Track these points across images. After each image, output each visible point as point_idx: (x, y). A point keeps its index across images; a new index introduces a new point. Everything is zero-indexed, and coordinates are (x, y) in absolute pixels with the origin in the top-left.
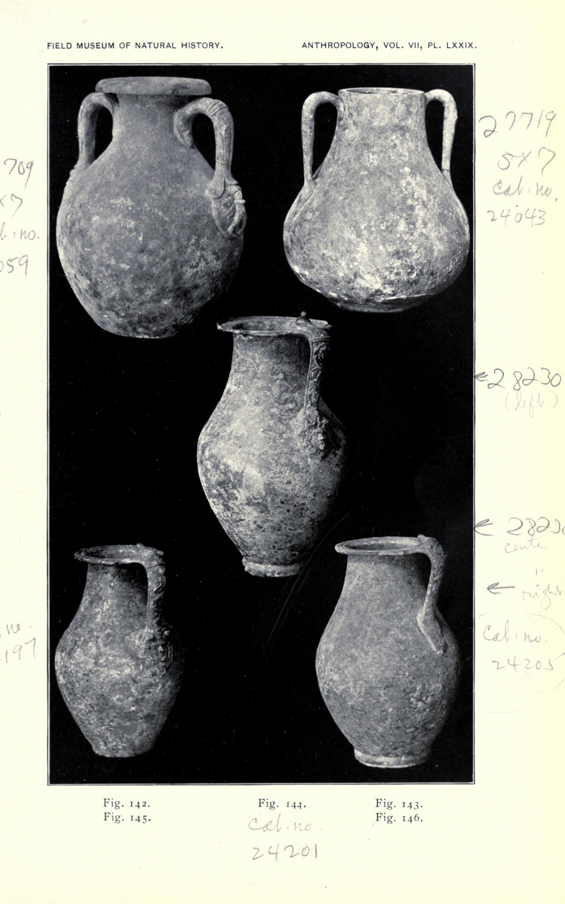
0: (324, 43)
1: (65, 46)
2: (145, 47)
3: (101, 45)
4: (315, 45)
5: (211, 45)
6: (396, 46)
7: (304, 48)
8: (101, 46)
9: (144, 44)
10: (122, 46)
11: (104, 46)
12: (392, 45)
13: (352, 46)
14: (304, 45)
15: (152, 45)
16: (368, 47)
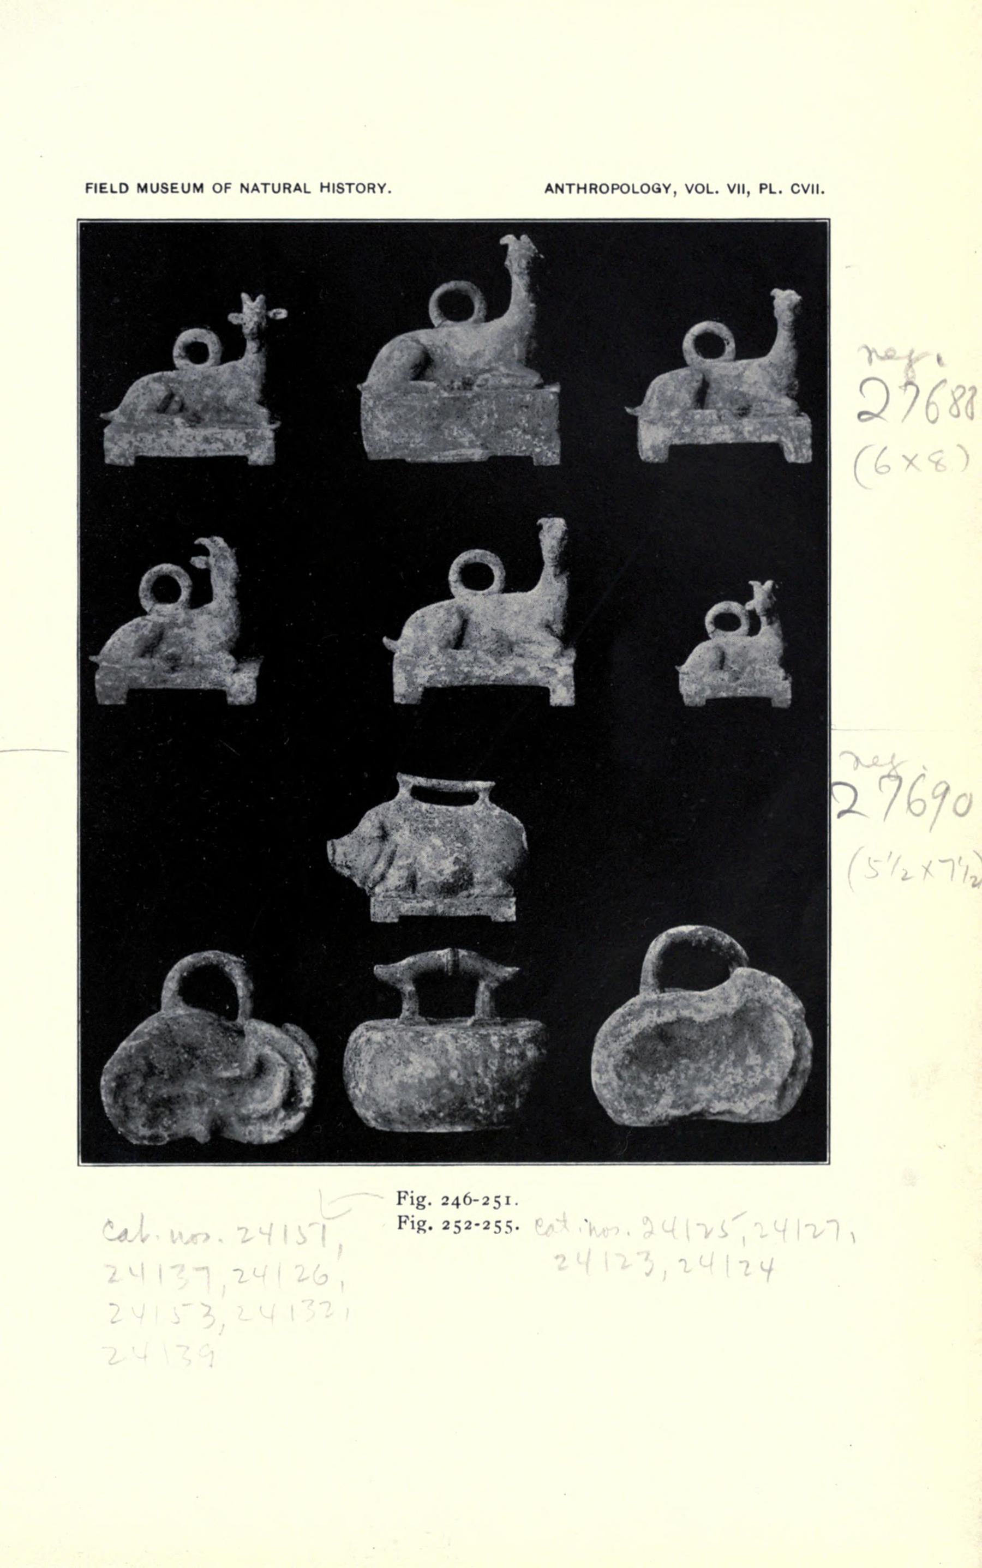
0: (582, 186)
1: (116, 188)
2: (257, 190)
3: (179, 187)
4: (566, 188)
5: (371, 187)
6: (706, 189)
7: (549, 192)
8: (179, 189)
9: (255, 185)
10: (218, 188)
11: (186, 189)
12: (700, 189)
13: (631, 189)
14: (549, 188)
15: (269, 188)
16: (659, 190)
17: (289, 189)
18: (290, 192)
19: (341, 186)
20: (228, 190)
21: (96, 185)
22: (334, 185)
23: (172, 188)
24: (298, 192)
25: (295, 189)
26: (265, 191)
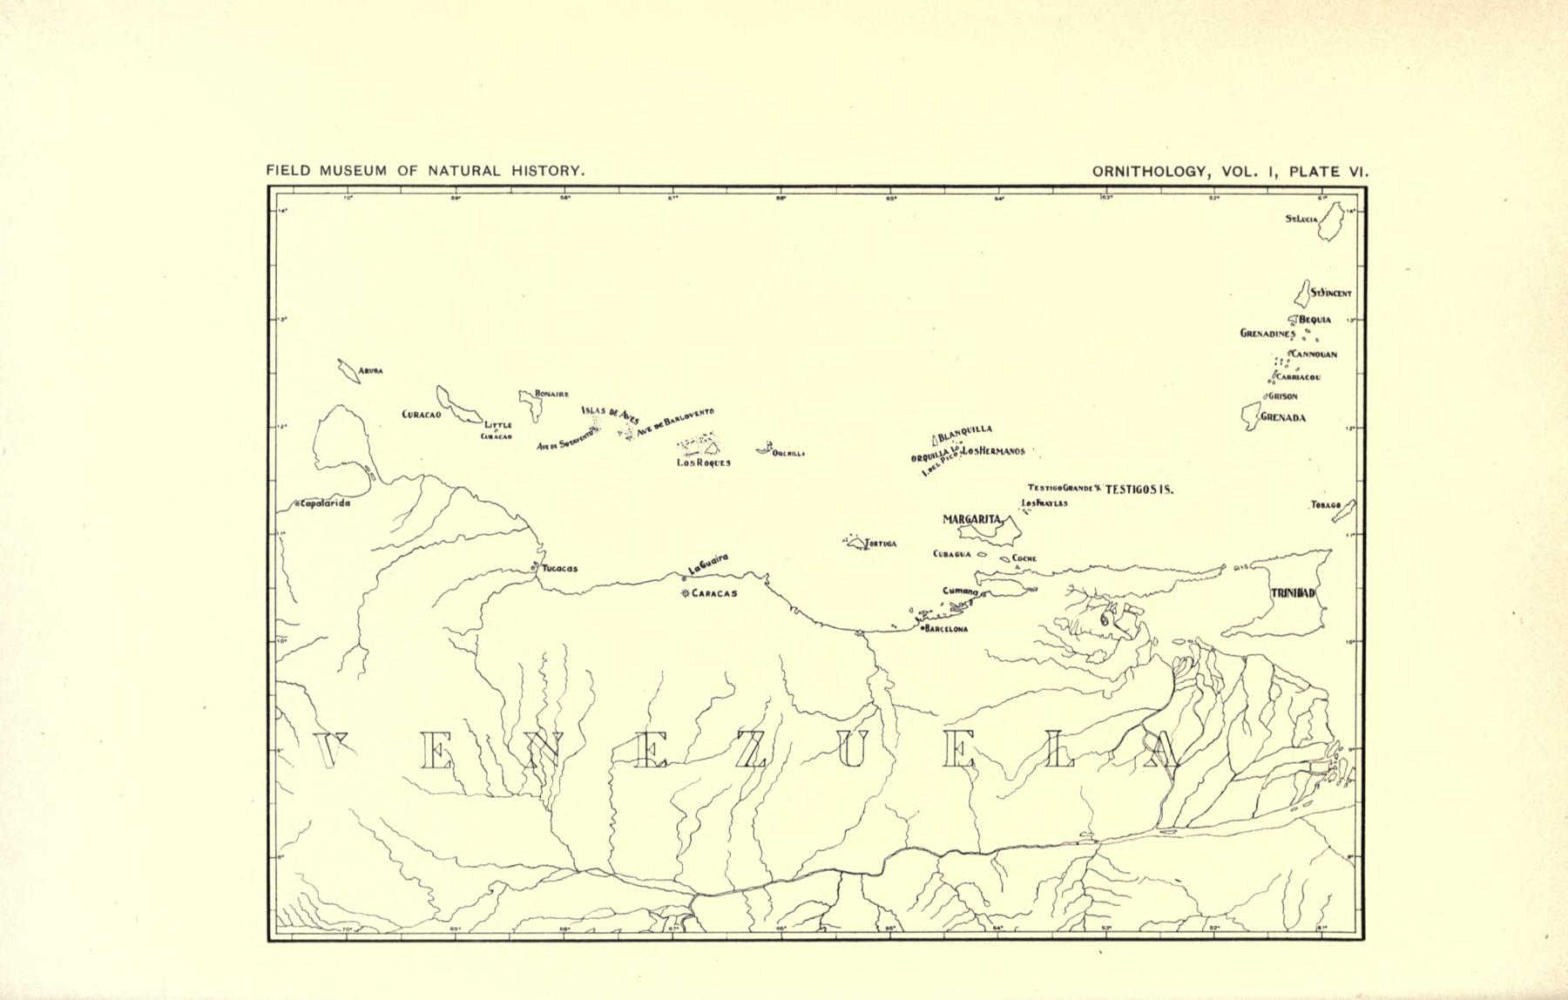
1: (297, 170)
2: (446, 172)
8: (363, 172)
9: (444, 167)
10: (403, 171)
11: (369, 171)
15: (458, 170)
17: (478, 171)
18: (479, 174)
19: (533, 168)
20: (413, 173)
21: (277, 167)
22: (526, 167)
23: (356, 171)
24: (487, 175)
25: (485, 172)
26: (454, 174)
